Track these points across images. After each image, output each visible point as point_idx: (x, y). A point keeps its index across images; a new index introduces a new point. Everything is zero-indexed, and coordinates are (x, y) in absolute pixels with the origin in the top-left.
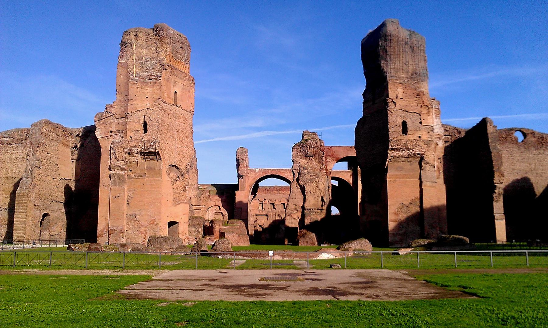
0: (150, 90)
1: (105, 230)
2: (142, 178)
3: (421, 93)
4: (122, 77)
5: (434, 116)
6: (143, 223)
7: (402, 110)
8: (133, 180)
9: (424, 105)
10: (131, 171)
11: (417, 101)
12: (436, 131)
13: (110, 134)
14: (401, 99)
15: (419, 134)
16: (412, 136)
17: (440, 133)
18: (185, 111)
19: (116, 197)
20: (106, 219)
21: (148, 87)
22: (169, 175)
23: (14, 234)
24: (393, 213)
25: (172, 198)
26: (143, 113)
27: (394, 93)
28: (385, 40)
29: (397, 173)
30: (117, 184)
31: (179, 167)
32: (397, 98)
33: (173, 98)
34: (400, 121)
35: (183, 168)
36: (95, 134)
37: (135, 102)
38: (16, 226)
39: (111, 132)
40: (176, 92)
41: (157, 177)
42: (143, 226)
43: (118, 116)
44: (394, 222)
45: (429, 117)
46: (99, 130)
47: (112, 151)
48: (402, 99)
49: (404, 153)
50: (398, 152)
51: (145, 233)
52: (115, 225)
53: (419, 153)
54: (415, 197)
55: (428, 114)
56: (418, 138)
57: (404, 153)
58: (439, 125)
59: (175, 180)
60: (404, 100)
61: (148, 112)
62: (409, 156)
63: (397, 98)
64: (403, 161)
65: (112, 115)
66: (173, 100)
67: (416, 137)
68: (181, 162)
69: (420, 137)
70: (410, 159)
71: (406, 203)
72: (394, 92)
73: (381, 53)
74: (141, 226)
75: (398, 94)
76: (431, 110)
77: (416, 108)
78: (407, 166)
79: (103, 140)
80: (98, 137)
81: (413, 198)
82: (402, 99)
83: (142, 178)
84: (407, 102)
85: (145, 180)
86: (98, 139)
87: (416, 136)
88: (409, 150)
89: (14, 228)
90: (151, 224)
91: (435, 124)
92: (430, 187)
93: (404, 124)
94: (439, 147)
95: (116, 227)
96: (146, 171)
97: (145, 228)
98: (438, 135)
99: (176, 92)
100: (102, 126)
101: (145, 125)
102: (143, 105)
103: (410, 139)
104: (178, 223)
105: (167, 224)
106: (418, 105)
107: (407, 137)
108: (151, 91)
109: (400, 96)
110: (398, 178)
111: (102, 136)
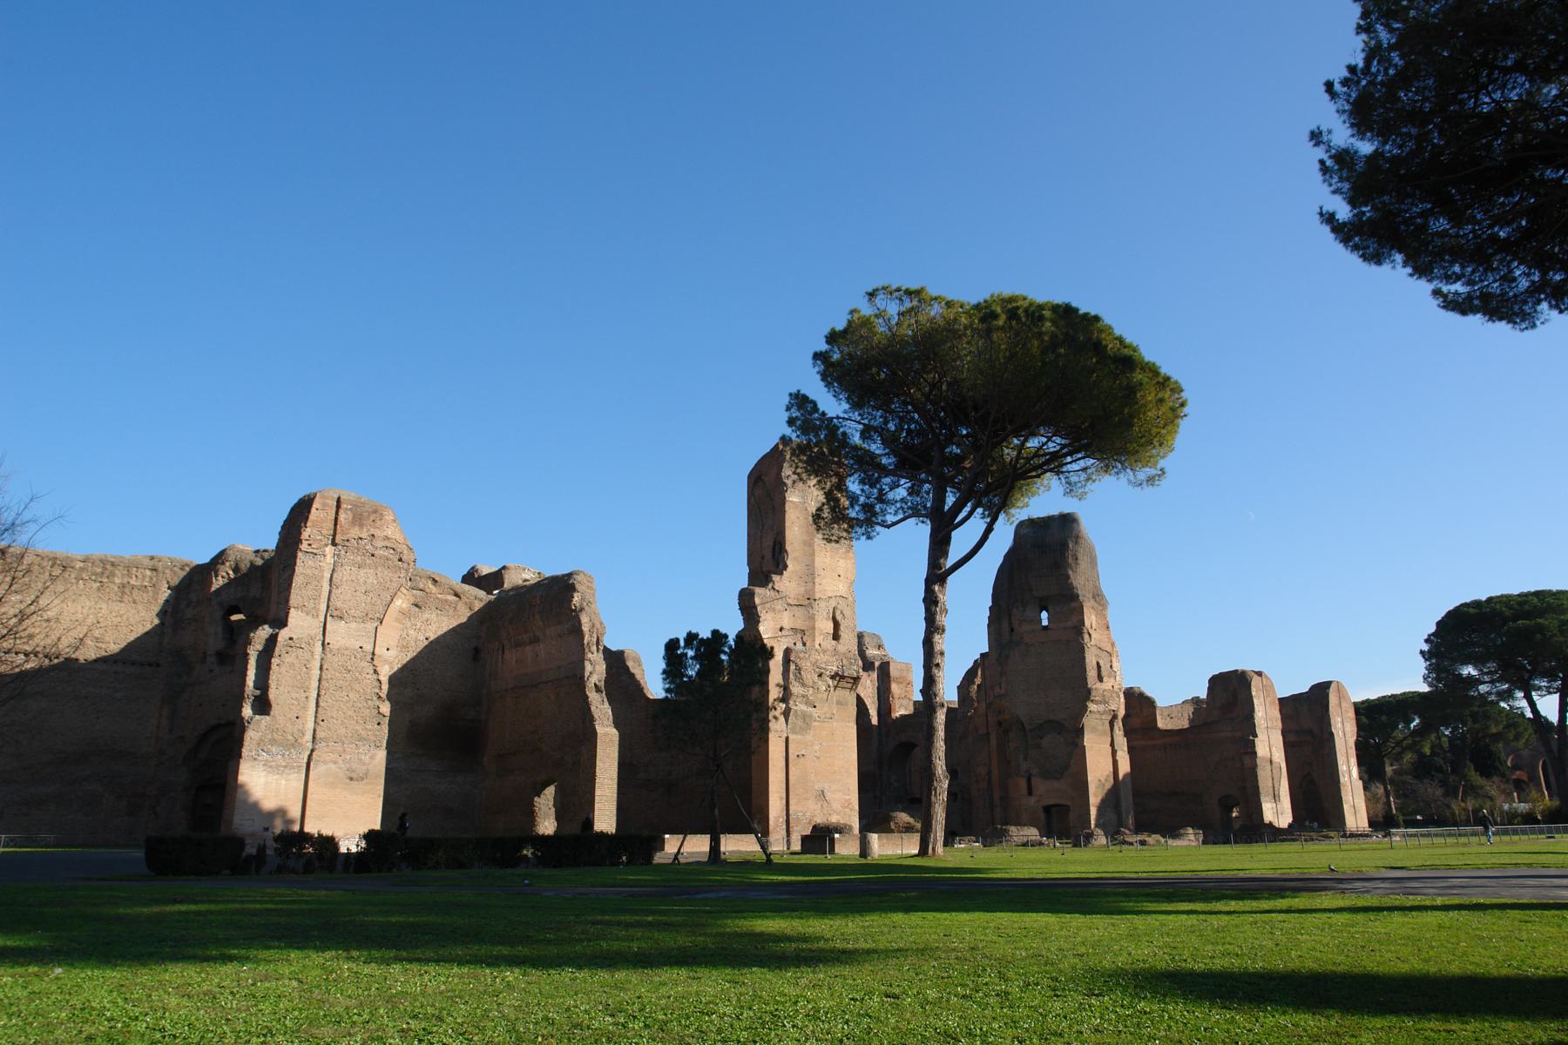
8: (817, 724)
19: (798, 756)
20: (781, 798)
26: (833, 603)
28: (1077, 543)
34: (1095, 663)
37: (824, 581)
38: (599, 809)
39: (781, 629)
42: (835, 812)
43: (790, 602)
47: (792, 667)
52: (800, 809)
71: (1103, 780)
73: (1070, 560)
89: (596, 813)
102: (835, 588)
109: (1094, 626)
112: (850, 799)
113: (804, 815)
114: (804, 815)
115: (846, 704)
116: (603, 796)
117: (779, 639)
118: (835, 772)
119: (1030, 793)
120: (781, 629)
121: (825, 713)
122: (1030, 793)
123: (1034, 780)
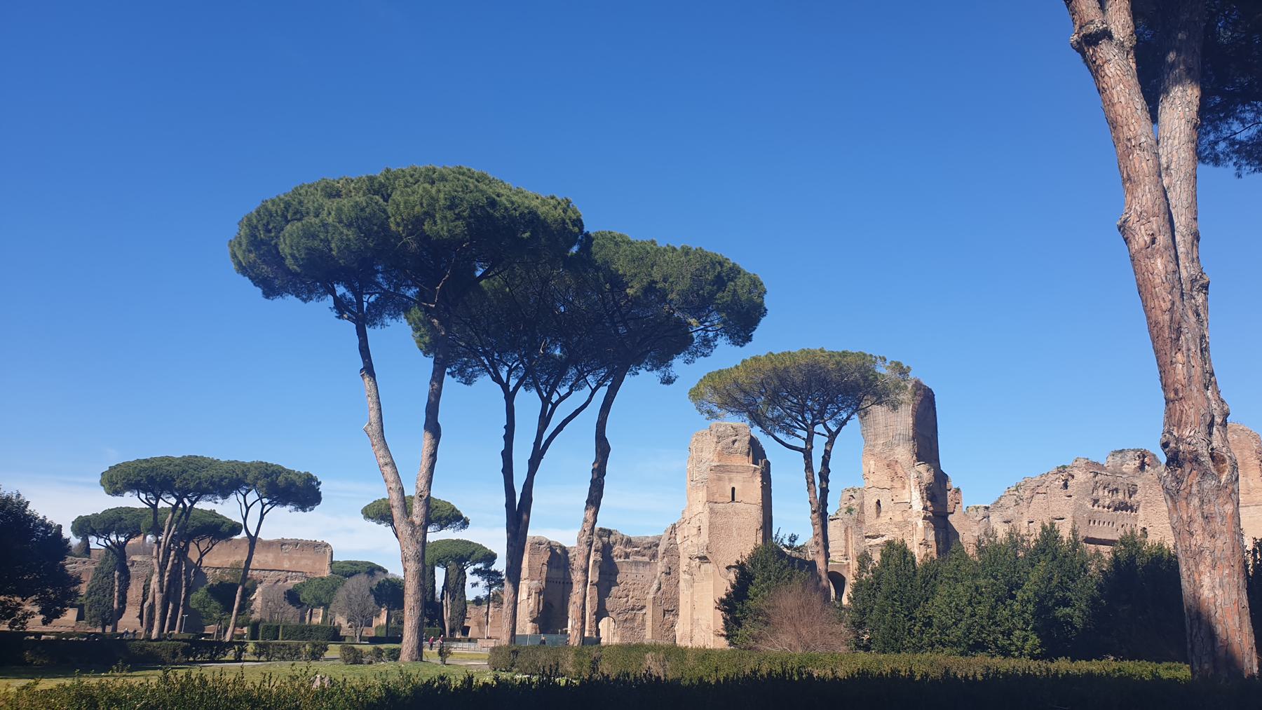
3: (893, 463)
5: (913, 488)
12: (914, 508)
15: (890, 514)
16: (884, 518)
40: (733, 489)
45: (904, 492)
50: (874, 540)
55: (904, 488)
76: (907, 481)
88: (883, 536)
91: (914, 498)
93: (878, 502)
99: (733, 489)
107: (879, 520)
109: (872, 470)
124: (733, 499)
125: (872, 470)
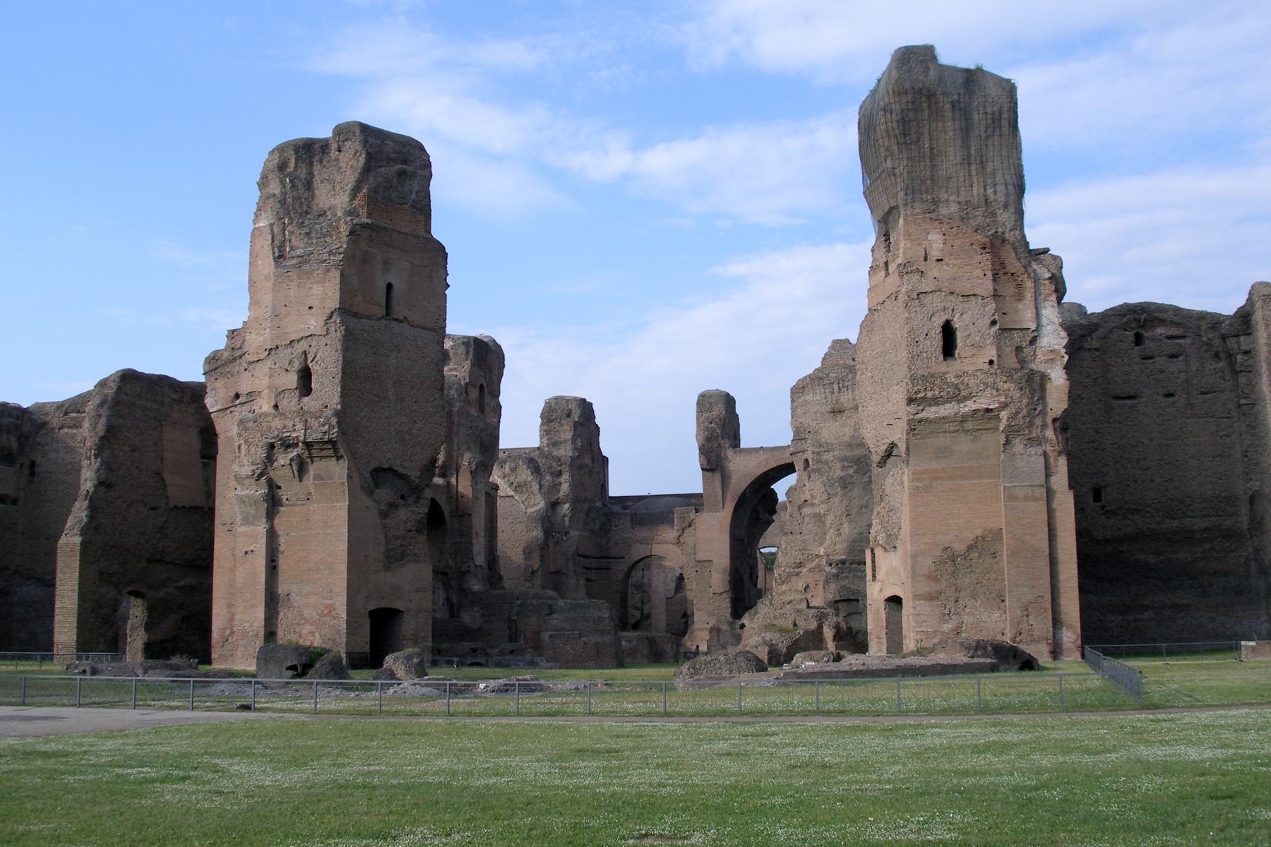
0: (317, 290)
1: (228, 632)
2: (303, 505)
4: (260, 262)
6: (306, 613)
7: (940, 291)
9: (1006, 273)
10: (280, 488)
11: (982, 265)
13: (237, 402)
14: (938, 260)
17: (1056, 347)
18: (419, 329)
19: (246, 553)
21: (312, 283)
22: (370, 493)
23: (55, 640)
24: (925, 575)
25: (382, 549)
27: (919, 248)
29: (934, 465)
30: (251, 519)
31: (401, 470)
32: (926, 259)
33: (383, 301)
34: (939, 321)
35: (414, 474)
36: (206, 401)
39: (237, 396)
40: (389, 286)
41: (338, 501)
42: (306, 621)
44: (926, 600)
46: (214, 392)
48: (942, 260)
49: (947, 410)
50: (933, 409)
51: (310, 638)
52: (246, 618)
53: (991, 407)
54: (985, 530)
56: (986, 366)
57: (947, 410)
58: (1054, 323)
59: (393, 506)
60: (947, 265)
61: (314, 343)
62: (964, 419)
63: (926, 259)
64: (950, 432)
65: (241, 357)
66: (381, 306)
67: (981, 362)
68: (408, 458)
69: (991, 362)
70: (969, 425)
71: (960, 547)
72: (920, 244)
74: (303, 621)
75: (931, 248)
77: (981, 284)
78: (964, 444)
79: (221, 415)
80: (210, 411)
81: (979, 532)
82: (942, 260)
83: (303, 505)
84: (956, 268)
85: (311, 507)
86: (212, 415)
87: (980, 361)
90: (325, 616)
92: (1026, 499)
94: (1056, 386)
95: (248, 624)
96: (313, 486)
97: (311, 624)
98: (1051, 351)
99: (389, 287)
100: (219, 384)
101: (305, 376)
103: (966, 369)
104: (402, 612)
105: (367, 615)
106: (985, 275)
108: (319, 292)
109: (935, 253)
110: (937, 478)
111: (219, 407)
112: (331, 605)
113: (251, 625)
114: (251, 625)
115: (330, 478)
116: (62, 607)
117: (231, 409)
118: (309, 570)
119: (874, 576)
120: (237, 396)
121: (297, 494)
122: (874, 576)
123: (878, 552)
124: (388, 314)
125: (935, 253)
